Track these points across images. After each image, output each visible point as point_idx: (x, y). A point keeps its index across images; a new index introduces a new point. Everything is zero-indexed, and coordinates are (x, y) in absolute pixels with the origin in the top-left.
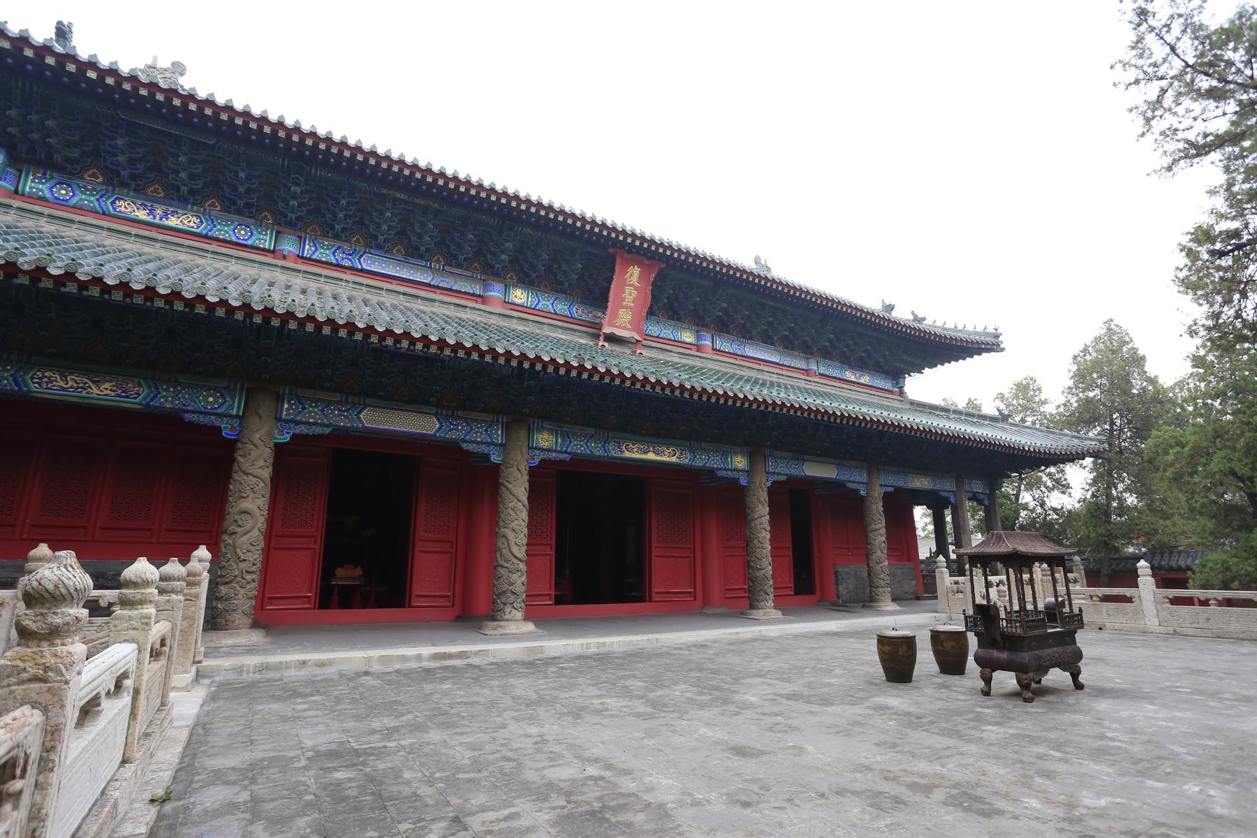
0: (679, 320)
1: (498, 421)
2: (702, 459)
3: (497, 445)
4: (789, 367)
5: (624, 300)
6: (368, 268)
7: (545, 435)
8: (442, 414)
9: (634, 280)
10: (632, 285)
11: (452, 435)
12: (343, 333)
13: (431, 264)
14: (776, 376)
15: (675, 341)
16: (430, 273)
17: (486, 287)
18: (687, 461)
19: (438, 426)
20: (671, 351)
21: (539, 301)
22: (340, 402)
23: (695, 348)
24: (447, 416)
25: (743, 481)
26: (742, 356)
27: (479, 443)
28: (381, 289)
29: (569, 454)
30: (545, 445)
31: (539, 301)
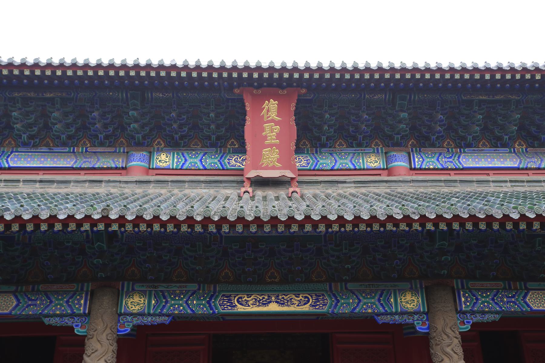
0: (360, 145)
1: (82, 289)
2: (348, 304)
3: (79, 315)
4: (539, 169)
5: (265, 138)
6: (15, 165)
7: (136, 299)
9: (273, 115)
10: (273, 121)
12: (184, 228)
13: (74, 150)
14: (509, 184)
15: (355, 169)
16: (73, 157)
17: (128, 160)
18: (325, 309)
19: (15, 304)
20: (345, 182)
21: (186, 160)
23: (386, 172)
25: (420, 327)
26: (456, 169)
27: (61, 316)
28: (18, 181)
29: (168, 315)
30: (135, 309)
31: (186, 160)
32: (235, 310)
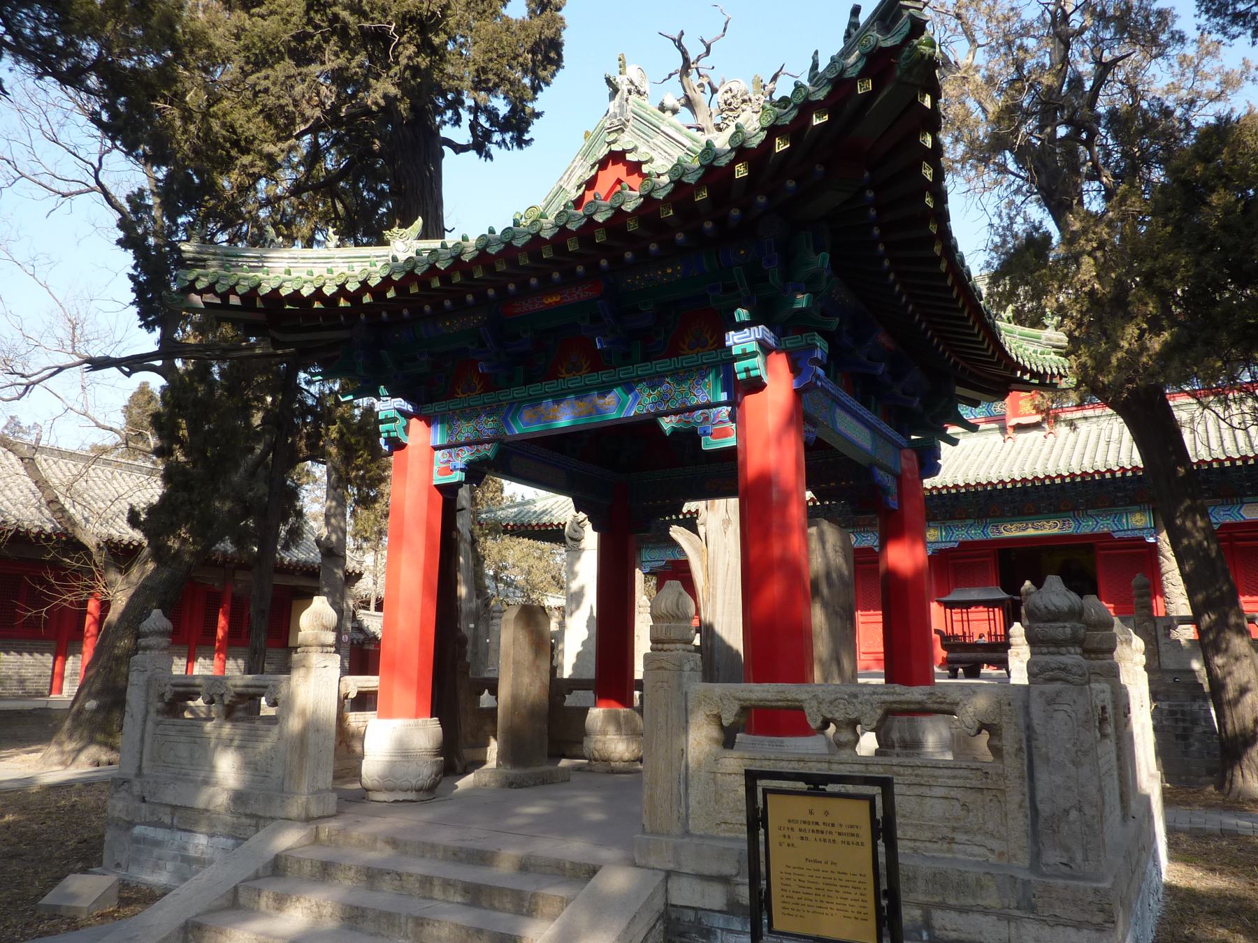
18: (1071, 530)
32: (1002, 536)
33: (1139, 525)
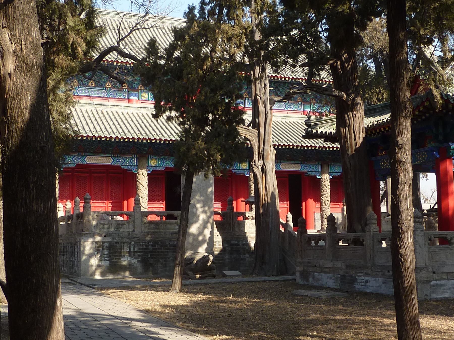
7: (154, 161)
8: (113, 157)
11: (117, 164)
17: (129, 95)
22: (78, 155)
24: (115, 157)
29: (164, 167)
30: (153, 165)
33: (244, 168)
